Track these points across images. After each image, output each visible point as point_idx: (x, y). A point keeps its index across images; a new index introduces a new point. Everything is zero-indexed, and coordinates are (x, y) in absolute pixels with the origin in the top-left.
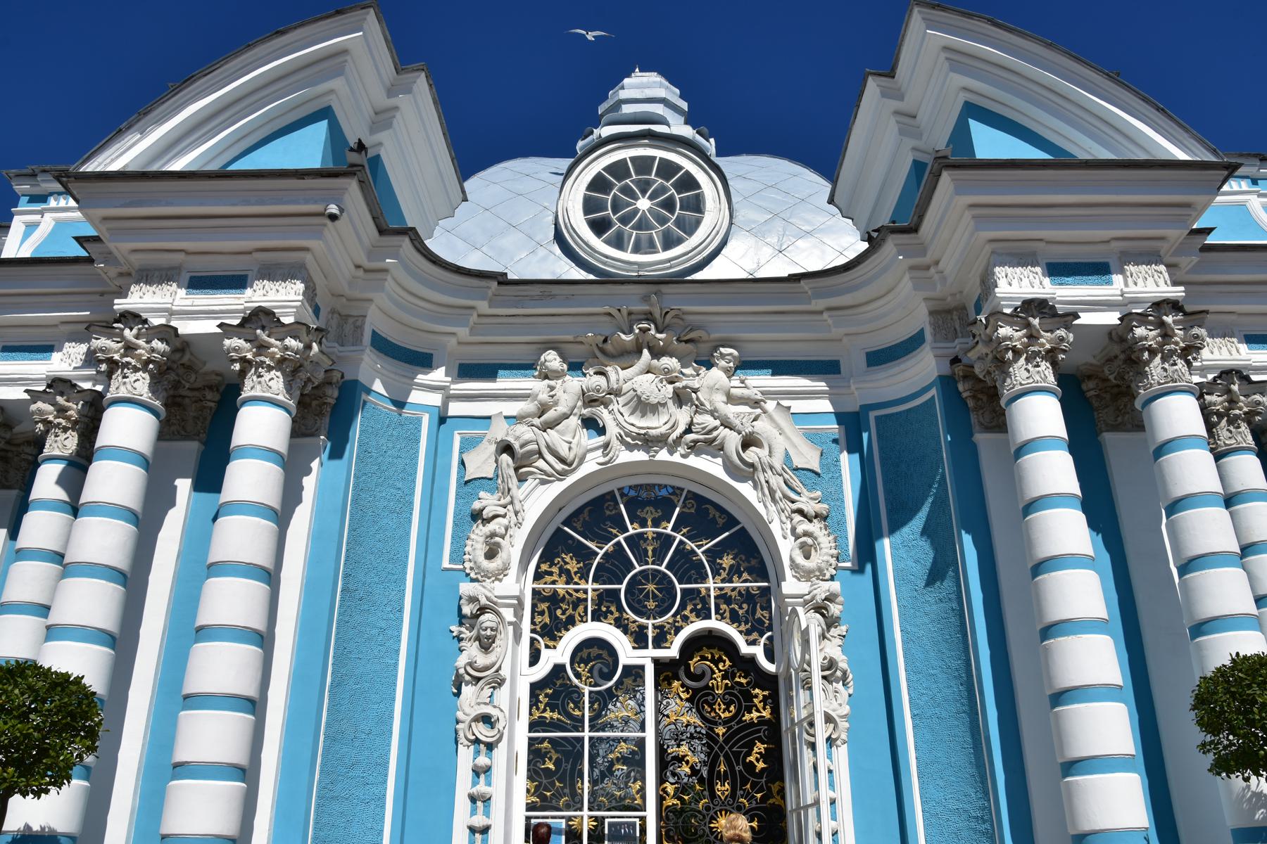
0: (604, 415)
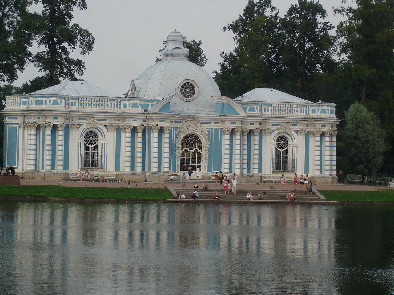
0: (189, 128)
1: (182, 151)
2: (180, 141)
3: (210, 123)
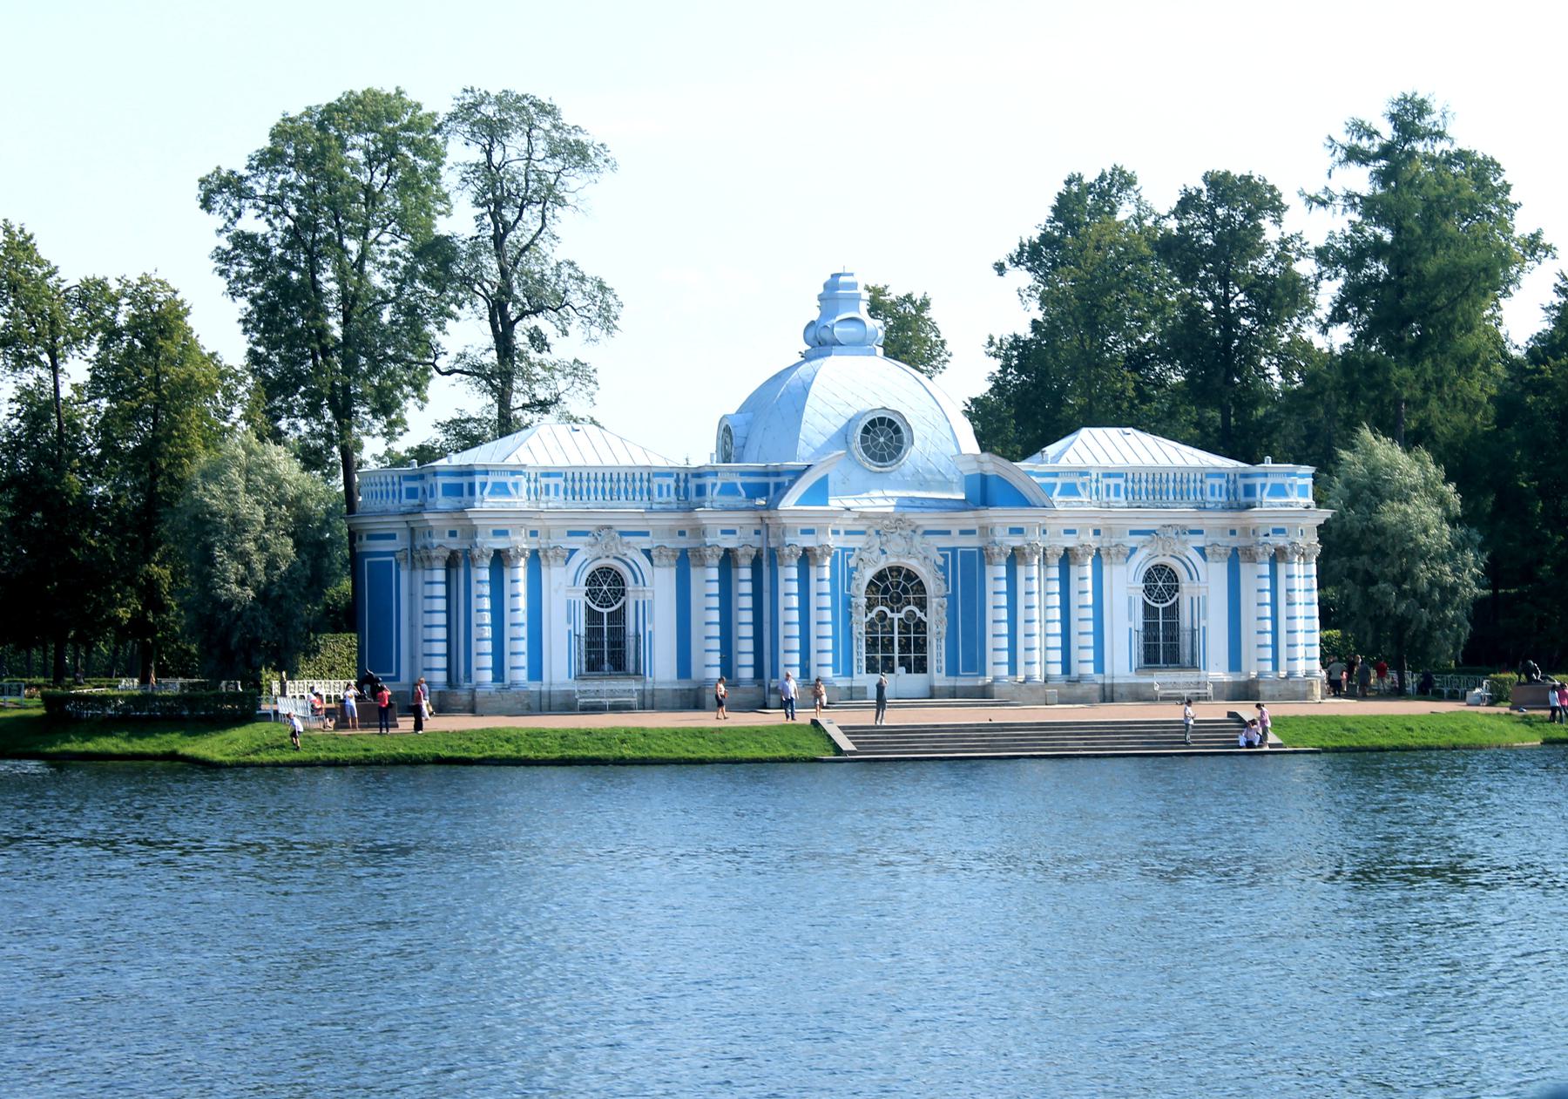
0: (887, 550)
1: (870, 615)
2: (864, 588)
3: (948, 533)
